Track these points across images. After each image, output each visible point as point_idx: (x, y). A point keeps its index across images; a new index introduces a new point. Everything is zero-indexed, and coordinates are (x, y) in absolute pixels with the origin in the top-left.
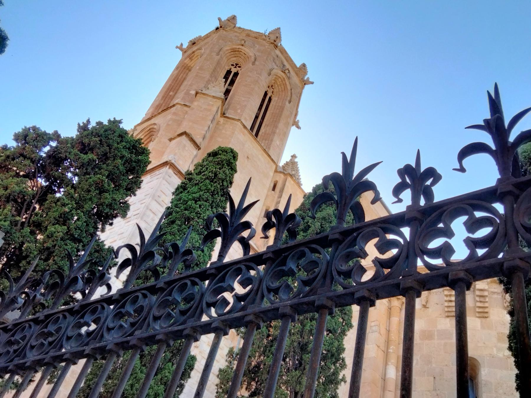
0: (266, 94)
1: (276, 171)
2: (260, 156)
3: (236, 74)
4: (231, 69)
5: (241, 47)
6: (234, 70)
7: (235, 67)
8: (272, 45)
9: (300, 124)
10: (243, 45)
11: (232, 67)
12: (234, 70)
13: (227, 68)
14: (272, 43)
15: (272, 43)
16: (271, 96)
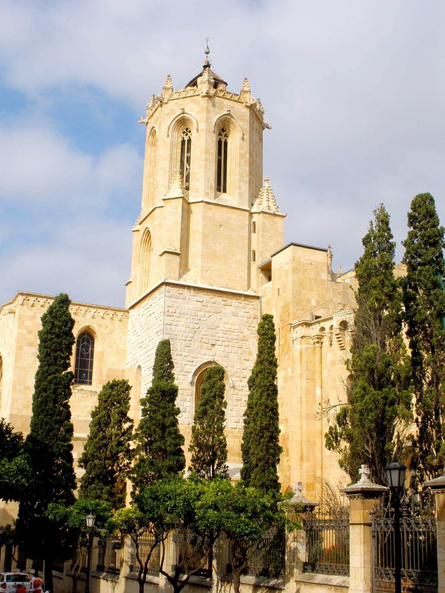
0: (220, 142)
1: (251, 214)
2: (232, 216)
3: (189, 141)
4: (183, 138)
5: (182, 115)
6: (186, 139)
7: (187, 135)
8: (206, 98)
9: (270, 125)
10: (183, 113)
11: (185, 136)
12: (186, 139)
13: (180, 140)
14: (205, 96)
15: (205, 96)
16: (226, 140)
